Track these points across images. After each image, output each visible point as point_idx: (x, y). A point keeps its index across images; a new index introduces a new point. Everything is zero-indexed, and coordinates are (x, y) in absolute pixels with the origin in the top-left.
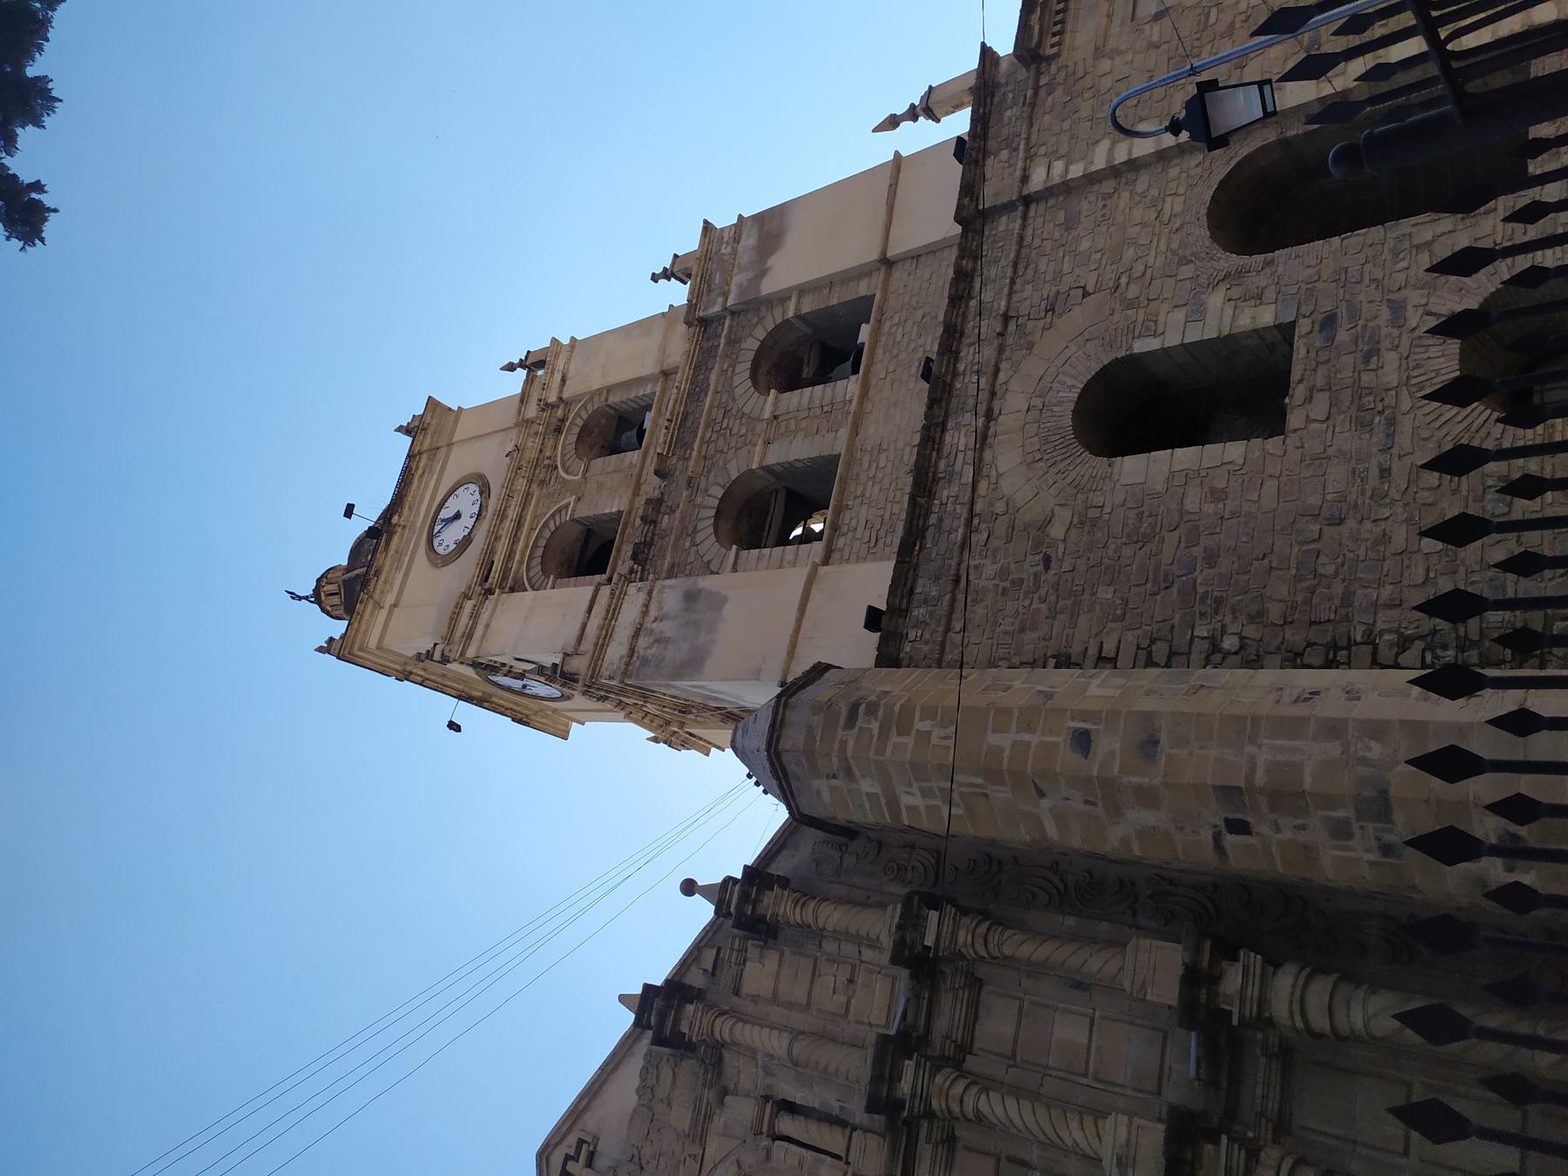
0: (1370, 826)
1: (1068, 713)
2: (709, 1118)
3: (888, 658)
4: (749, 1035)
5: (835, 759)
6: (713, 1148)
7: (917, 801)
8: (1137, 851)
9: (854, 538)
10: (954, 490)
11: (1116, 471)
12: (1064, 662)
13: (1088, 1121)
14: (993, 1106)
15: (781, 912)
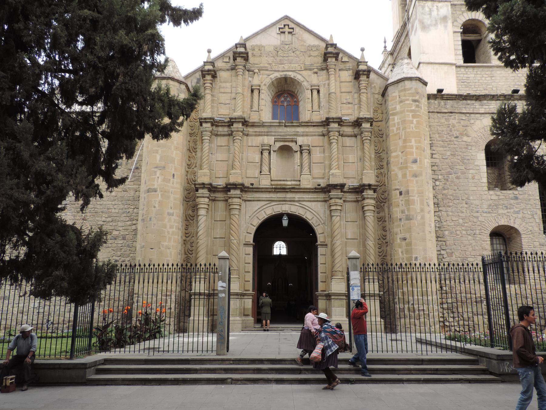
0: (404, 217)
1: (420, 157)
2: (310, 70)
3: (429, 97)
4: (332, 78)
5: (404, 98)
6: (305, 73)
7: (396, 121)
8: (392, 173)
9: (464, 74)
10: (477, 107)
11: (481, 152)
12: (431, 145)
13: (337, 166)
14: (334, 146)
15: (362, 82)
